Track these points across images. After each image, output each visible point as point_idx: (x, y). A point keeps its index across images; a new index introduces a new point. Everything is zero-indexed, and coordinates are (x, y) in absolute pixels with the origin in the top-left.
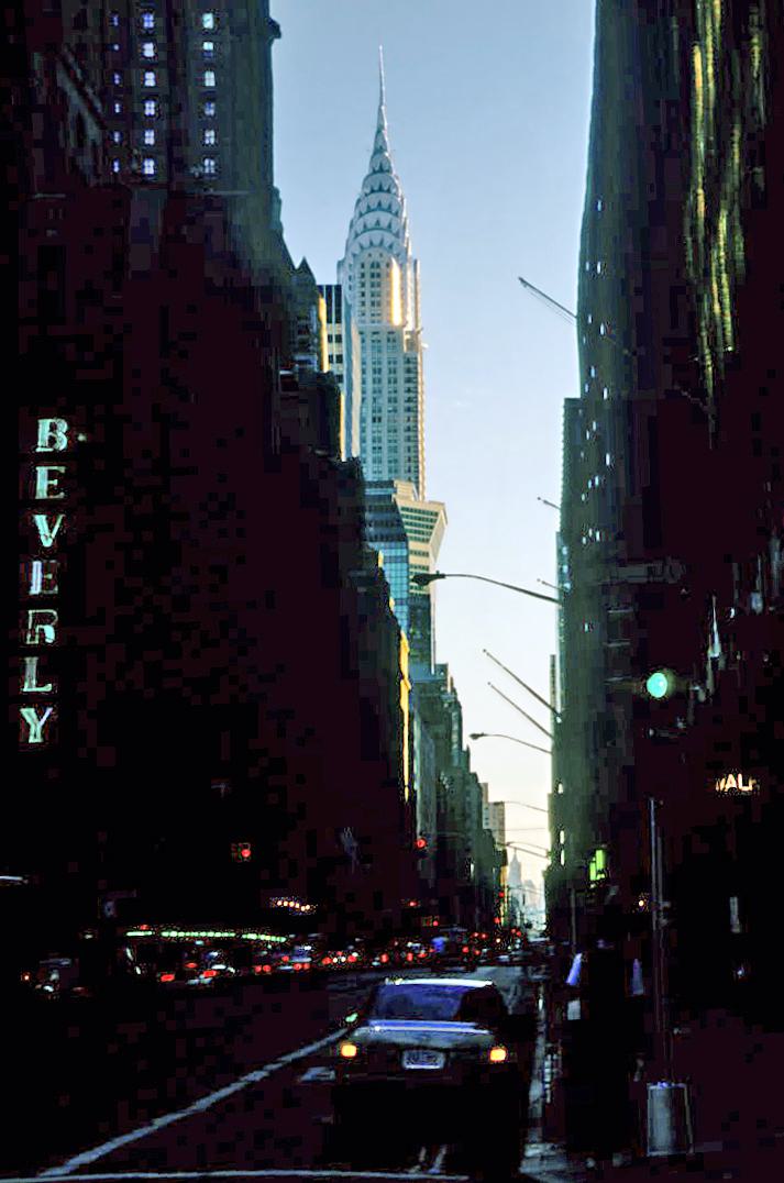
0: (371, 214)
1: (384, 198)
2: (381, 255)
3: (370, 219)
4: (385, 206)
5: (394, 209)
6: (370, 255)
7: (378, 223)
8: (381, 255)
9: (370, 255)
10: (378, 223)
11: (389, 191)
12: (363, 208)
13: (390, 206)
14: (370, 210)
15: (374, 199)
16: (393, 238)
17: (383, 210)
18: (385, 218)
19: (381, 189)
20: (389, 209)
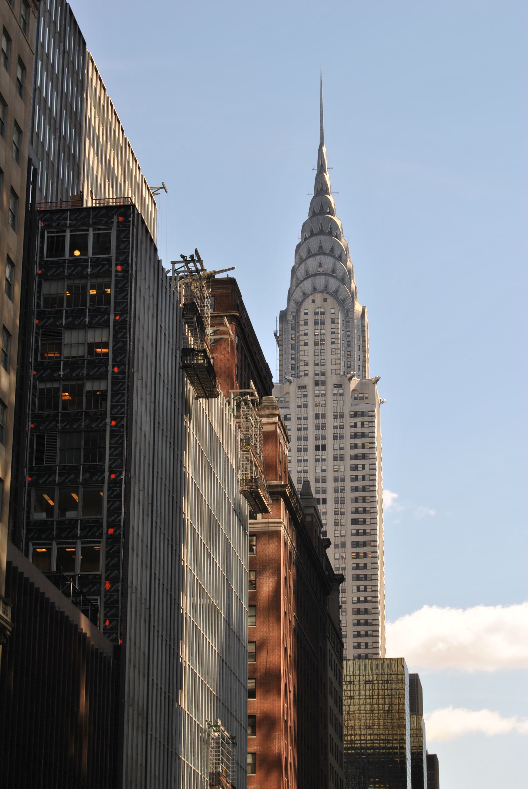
0: (311, 259)
1: (326, 242)
2: (325, 300)
3: (312, 264)
4: (327, 248)
5: (337, 253)
6: (313, 301)
7: (320, 265)
8: (325, 300)
9: (313, 301)
10: (320, 265)
11: (330, 234)
12: (303, 253)
13: (332, 250)
14: (310, 255)
15: (314, 244)
16: (338, 283)
17: (325, 254)
18: (328, 263)
19: (321, 232)
20: (331, 253)
